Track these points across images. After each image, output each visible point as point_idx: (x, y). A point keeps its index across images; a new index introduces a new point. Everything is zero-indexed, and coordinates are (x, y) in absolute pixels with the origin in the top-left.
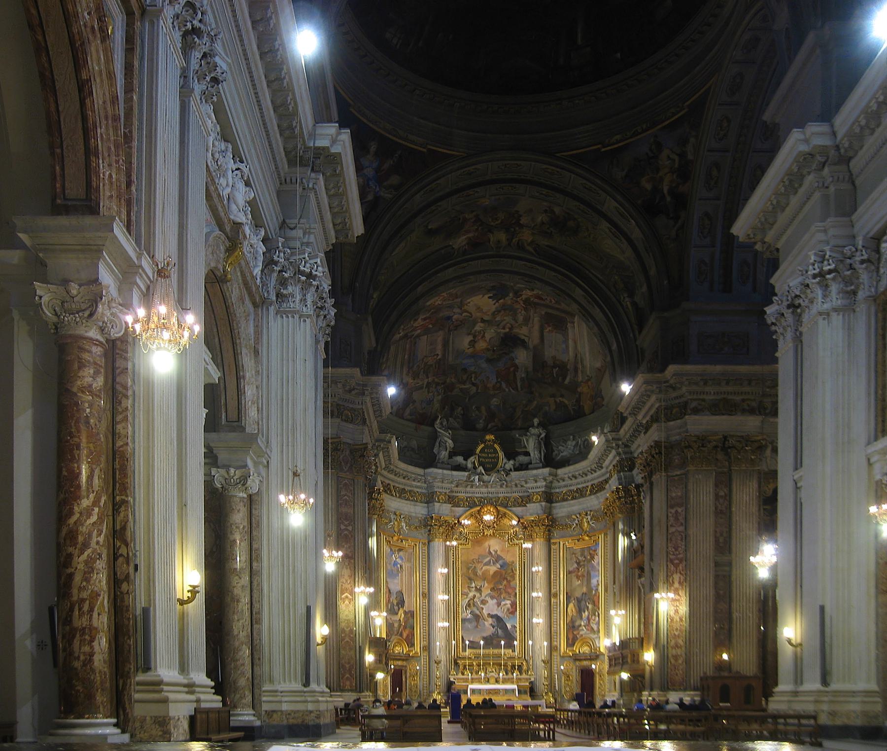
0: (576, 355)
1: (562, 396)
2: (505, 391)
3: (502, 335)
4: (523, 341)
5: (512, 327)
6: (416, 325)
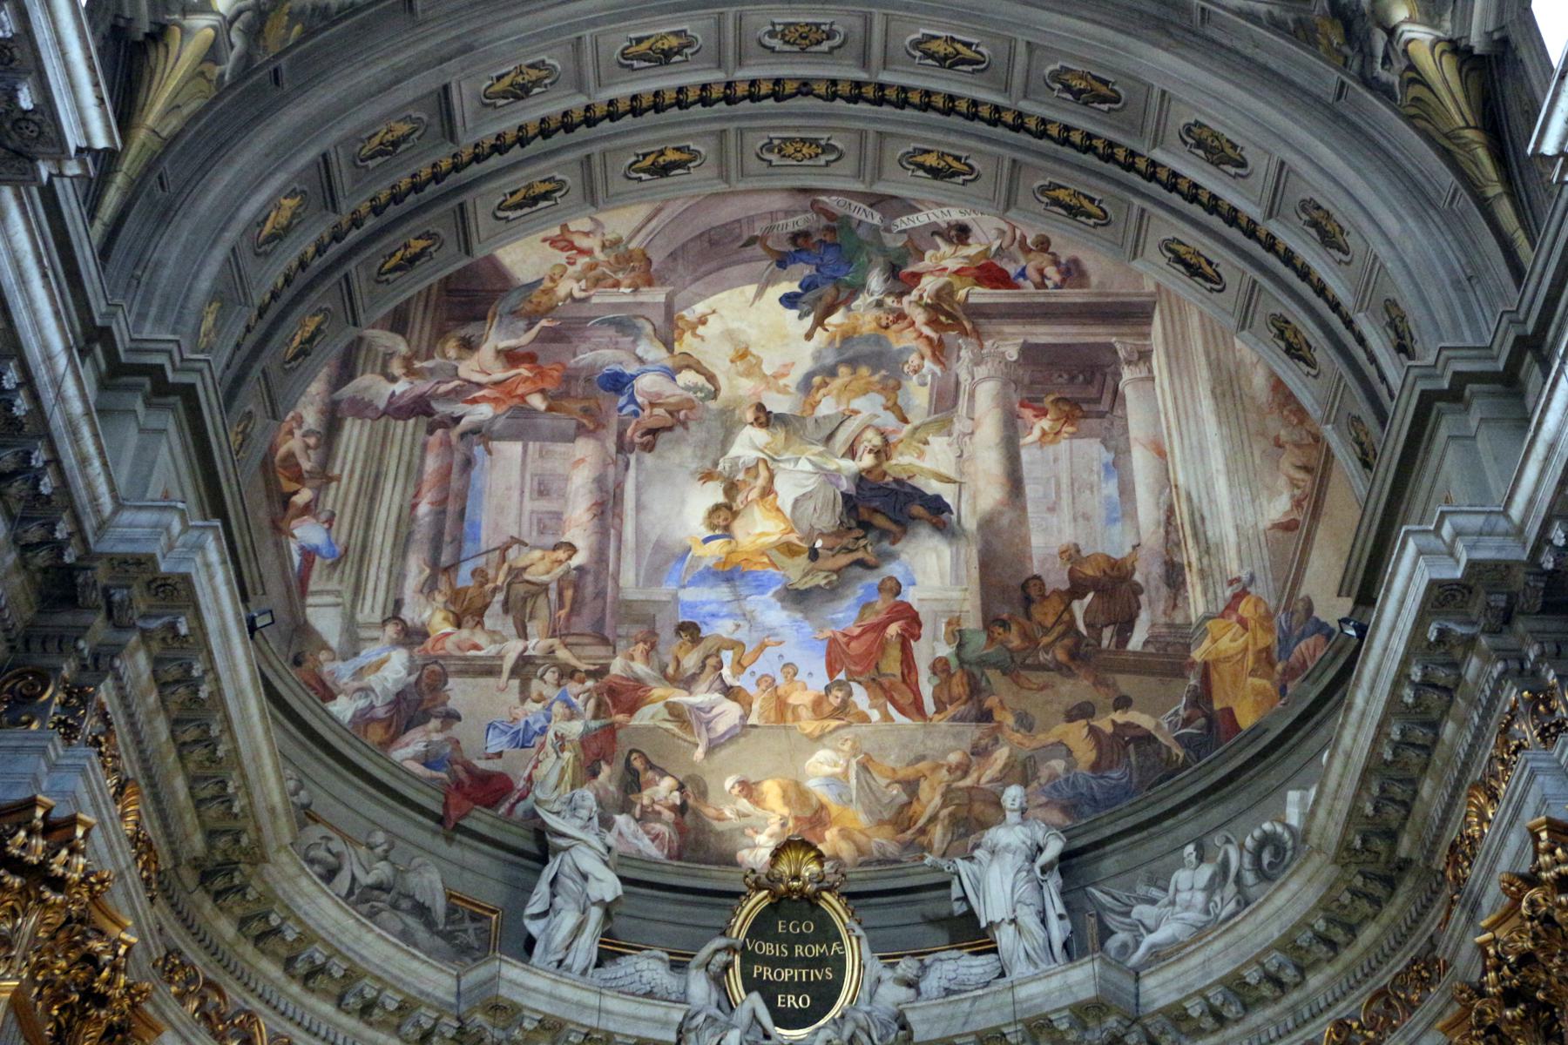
0: (1171, 511)
1: (1123, 703)
2: (865, 719)
3: (846, 485)
4: (937, 507)
5: (886, 442)
6: (469, 369)
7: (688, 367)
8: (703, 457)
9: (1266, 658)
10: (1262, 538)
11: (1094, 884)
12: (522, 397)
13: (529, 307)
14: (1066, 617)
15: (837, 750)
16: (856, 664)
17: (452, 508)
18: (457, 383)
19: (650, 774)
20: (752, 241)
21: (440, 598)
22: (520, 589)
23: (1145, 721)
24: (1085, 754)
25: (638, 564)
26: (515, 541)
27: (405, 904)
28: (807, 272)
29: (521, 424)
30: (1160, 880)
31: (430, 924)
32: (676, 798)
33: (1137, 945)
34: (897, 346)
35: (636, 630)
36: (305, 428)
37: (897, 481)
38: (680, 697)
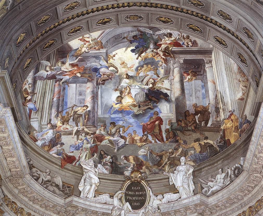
0: (216, 96)
1: (206, 138)
2: (151, 142)
3: (146, 91)
4: (166, 96)
5: (155, 81)
6: (64, 68)
7: (111, 66)
8: (115, 86)
9: (237, 128)
10: (236, 102)
11: (200, 177)
12: (75, 74)
13: (76, 54)
14: (194, 119)
15: (145, 149)
16: (149, 130)
17: (61, 98)
18: (61, 71)
19: (105, 155)
20: (124, 38)
21: (59, 119)
22: (76, 116)
23: (211, 142)
24: (198, 149)
25: (102, 109)
26: (75, 105)
27: (54, 185)
28: (137, 45)
29: (75, 80)
30: (214, 176)
31: (59, 189)
32: (111, 160)
33: (209, 191)
34: (157, 60)
35: (101, 124)
36: (29, 83)
37: (157, 90)
38: (111, 138)
